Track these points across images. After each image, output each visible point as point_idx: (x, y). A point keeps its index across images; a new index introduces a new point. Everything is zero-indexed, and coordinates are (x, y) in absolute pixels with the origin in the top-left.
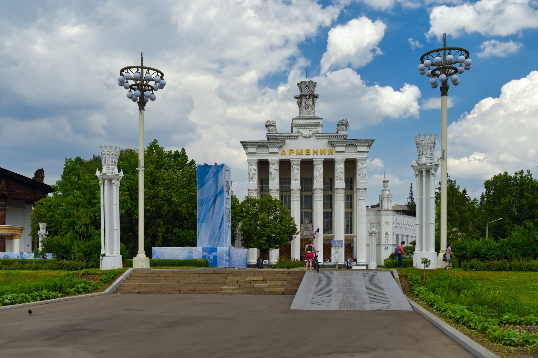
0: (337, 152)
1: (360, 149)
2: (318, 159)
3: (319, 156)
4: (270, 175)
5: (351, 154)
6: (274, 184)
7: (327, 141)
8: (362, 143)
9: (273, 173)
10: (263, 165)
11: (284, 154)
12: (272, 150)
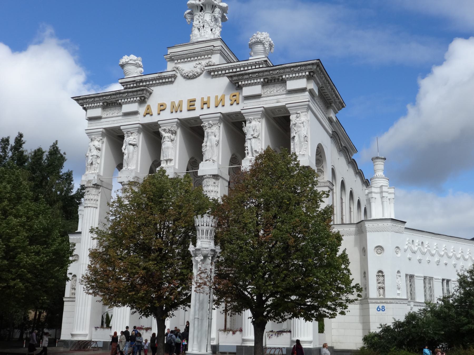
0: (247, 98)
1: (291, 85)
2: (207, 113)
3: (213, 110)
5: (274, 98)
12: (126, 108)
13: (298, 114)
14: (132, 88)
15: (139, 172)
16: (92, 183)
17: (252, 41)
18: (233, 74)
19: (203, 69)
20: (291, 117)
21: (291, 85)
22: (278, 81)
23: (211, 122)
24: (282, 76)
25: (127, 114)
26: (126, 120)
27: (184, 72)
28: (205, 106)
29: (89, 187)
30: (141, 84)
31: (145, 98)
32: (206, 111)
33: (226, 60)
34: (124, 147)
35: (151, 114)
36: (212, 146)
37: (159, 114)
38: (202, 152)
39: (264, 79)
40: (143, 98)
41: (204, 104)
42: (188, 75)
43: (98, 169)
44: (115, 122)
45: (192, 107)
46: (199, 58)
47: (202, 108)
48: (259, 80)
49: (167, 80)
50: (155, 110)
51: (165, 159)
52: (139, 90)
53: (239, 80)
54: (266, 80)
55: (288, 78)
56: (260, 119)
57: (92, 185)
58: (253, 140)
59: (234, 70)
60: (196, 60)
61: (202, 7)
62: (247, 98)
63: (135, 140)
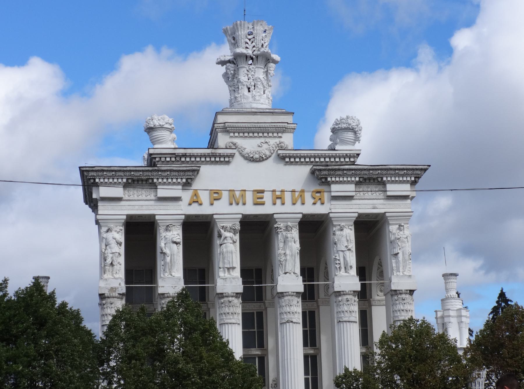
1: (393, 189)
2: (288, 213)
3: (288, 208)
4: (159, 256)
5: (369, 203)
6: (171, 280)
7: (306, 170)
8: (399, 175)
9: (167, 251)
10: (141, 234)
11: (195, 200)
16: (117, 292)
17: (340, 126)
18: (324, 168)
19: (272, 151)
23: (289, 224)
26: (162, 207)
28: (278, 202)
29: (113, 297)
35: (200, 202)
37: (212, 204)
39: (359, 178)
41: (277, 198)
42: (252, 157)
44: (144, 208)
46: (266, 134)
47: (274, 204)
48: (353, 179)
51: (228, 267)
52: (188, 171)
53: (329, 175)
56: (351, 226)
57: (117, 295)
63: (178, 237)
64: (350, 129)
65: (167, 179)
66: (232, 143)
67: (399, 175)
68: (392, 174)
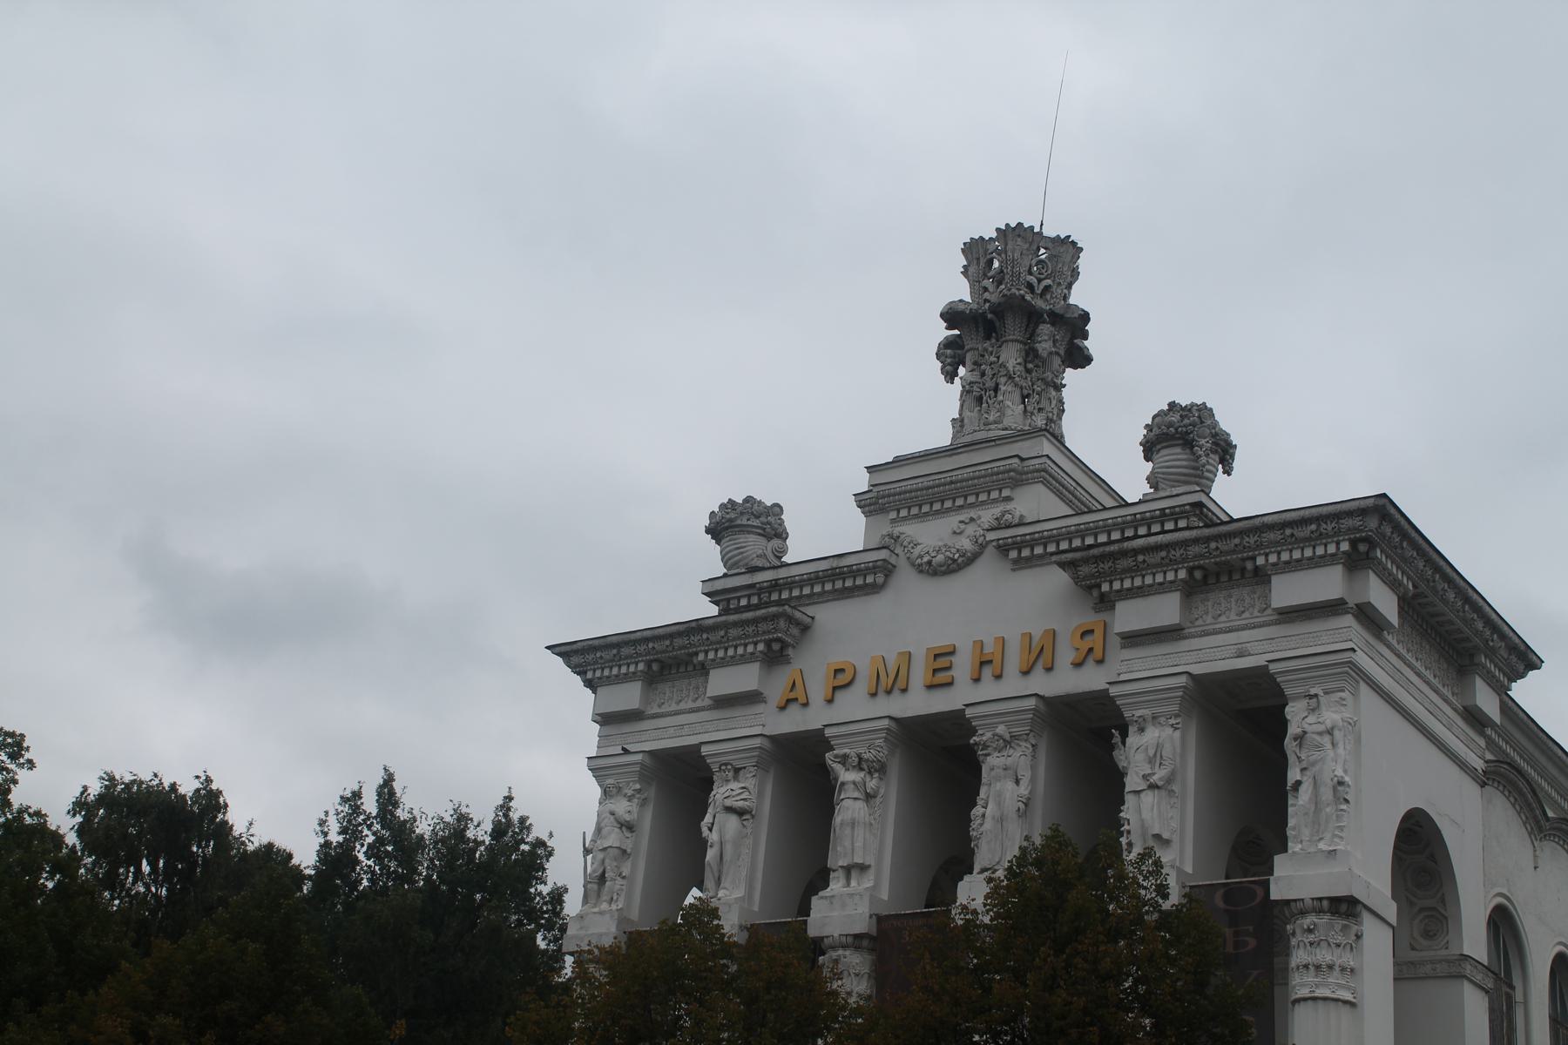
0: (1133, 639)
3: (1014, 684)
12: (723, 682)
13: (1311, 697)
14: (748, 608)
15: (756, 909)
18: (1078, 555)
20: (1287, 709)
21: (1289, 590)
22: (1243, 577)
23: (1001, 729)
24: (1254, 559)
25: (723, 702)
27: (916, 552)
30: (775, 597)
31: (784, 645)
32: (988, 689)
33: (1069, 503)
34: (708, 818)
35: (802, 700)
36: (1001, 820)
37: (830, 701)
38: (969, 839)
39: (1191, 571)
40: (776, 646)
41: (982, 663)
42: (929, 563)
43: (622, 899)
44: (686, 730)
45: (942, 677)
49: (859, 581)
50: (817, 689)
52: (765, 619)
53: (1100, 574)
54: (1198, 575)
55: (1274, 565)
56: (1177, 716)
58: (1148, 798)
59: (1089, 541)
60: (961, 507)
61: (991, 322)
62: (1133, 639)
64: (1172, 437)
65: (726, 649)
66: (890, 536)
67: (1298, 541)
68: (1277, 543)
